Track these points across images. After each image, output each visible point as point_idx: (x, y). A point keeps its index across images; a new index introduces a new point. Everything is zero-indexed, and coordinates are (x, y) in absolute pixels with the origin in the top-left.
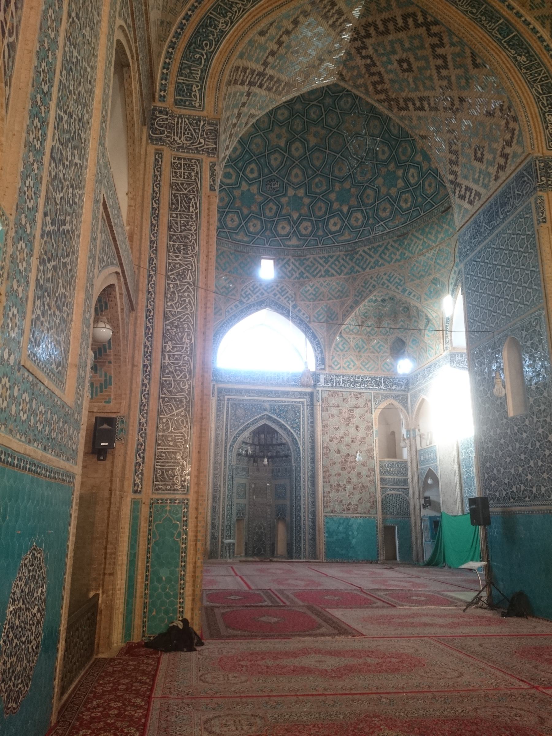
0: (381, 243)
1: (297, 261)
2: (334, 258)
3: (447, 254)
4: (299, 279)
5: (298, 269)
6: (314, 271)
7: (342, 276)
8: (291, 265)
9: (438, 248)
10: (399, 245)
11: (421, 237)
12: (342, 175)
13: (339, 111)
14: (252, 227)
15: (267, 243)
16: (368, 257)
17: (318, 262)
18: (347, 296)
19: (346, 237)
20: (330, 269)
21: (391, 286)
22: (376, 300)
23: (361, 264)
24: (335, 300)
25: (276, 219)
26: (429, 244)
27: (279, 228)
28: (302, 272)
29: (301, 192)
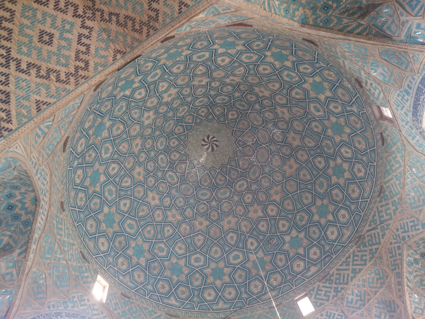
0: (373, 214)
1: (326, 283)
2: (351, 256)
3: (418, 161)
4: (336, 295)
5: (331, 288)
6: (344, 280)
7: (368, 264)
8: (323, 289)
9: (407, 167)
10: (385, 200)
11: (390, 177)
12: (310, 200)
13: (277, 169)
14: (274, 282)
15: (293, 285)
16: (373, 232)
17: (342, 270)
18: (387, 277)
19: (347, 233)
20: (355, 267)
21: (410, 233)
22: (415, 260)
23: (374, 241)
24: (382, 290)
25: (289, 263)
26: (400, 173)
27: (296, 269)
28: (335, 288)
29: (294, 233)
